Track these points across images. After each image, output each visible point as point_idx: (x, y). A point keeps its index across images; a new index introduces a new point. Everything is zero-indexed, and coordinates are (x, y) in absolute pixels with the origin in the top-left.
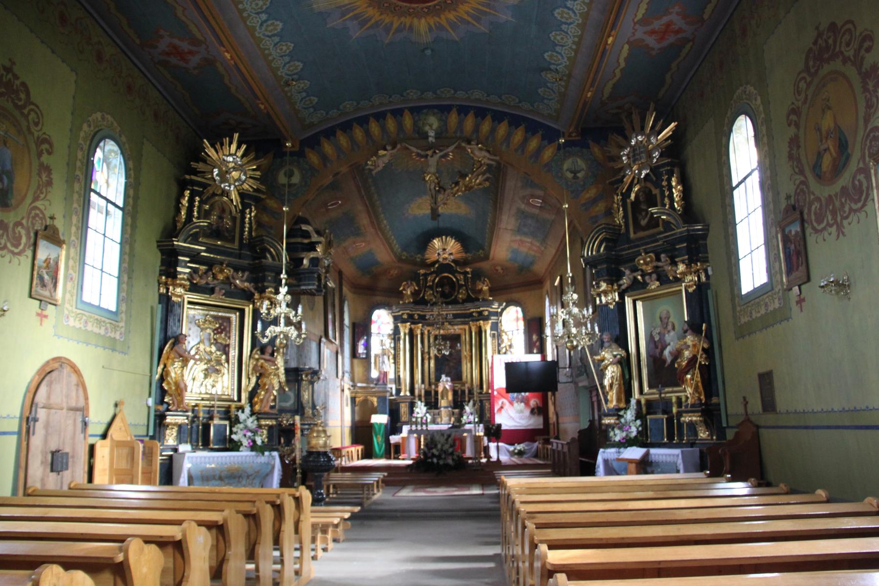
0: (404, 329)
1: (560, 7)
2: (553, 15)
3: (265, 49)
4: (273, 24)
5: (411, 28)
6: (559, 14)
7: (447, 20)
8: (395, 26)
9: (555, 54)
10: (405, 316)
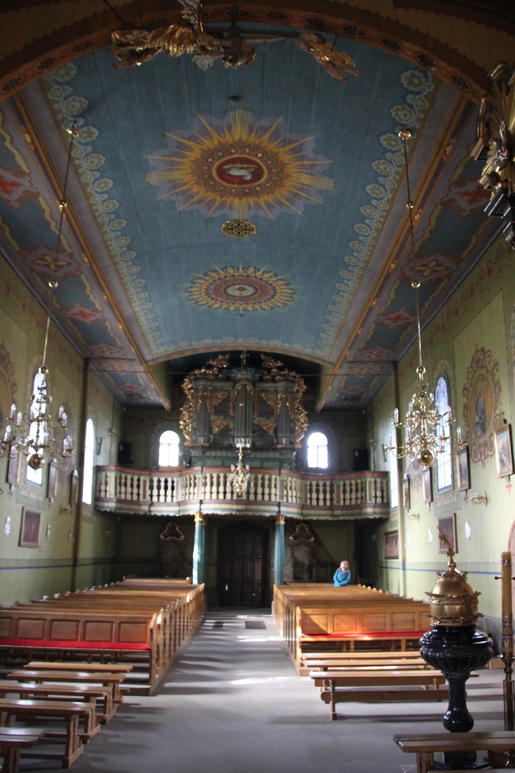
1: (111, 189)
2: (113, 180)
3: (396, 180)
4: (373, 193)
5: (251, 131)
6: (109, 183)
7: (212, 139)
8: (266, 136)
9: (89, 140)
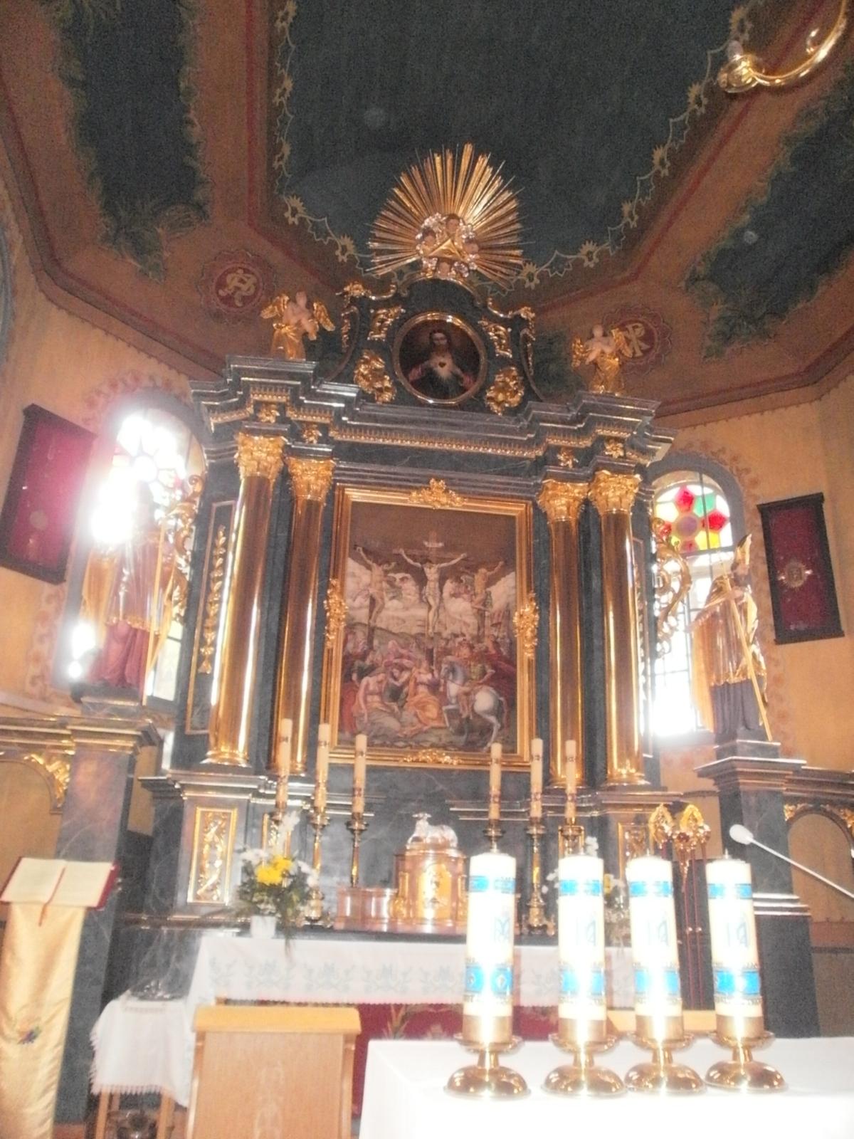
0: (257, 455)
10: (270, 417)
